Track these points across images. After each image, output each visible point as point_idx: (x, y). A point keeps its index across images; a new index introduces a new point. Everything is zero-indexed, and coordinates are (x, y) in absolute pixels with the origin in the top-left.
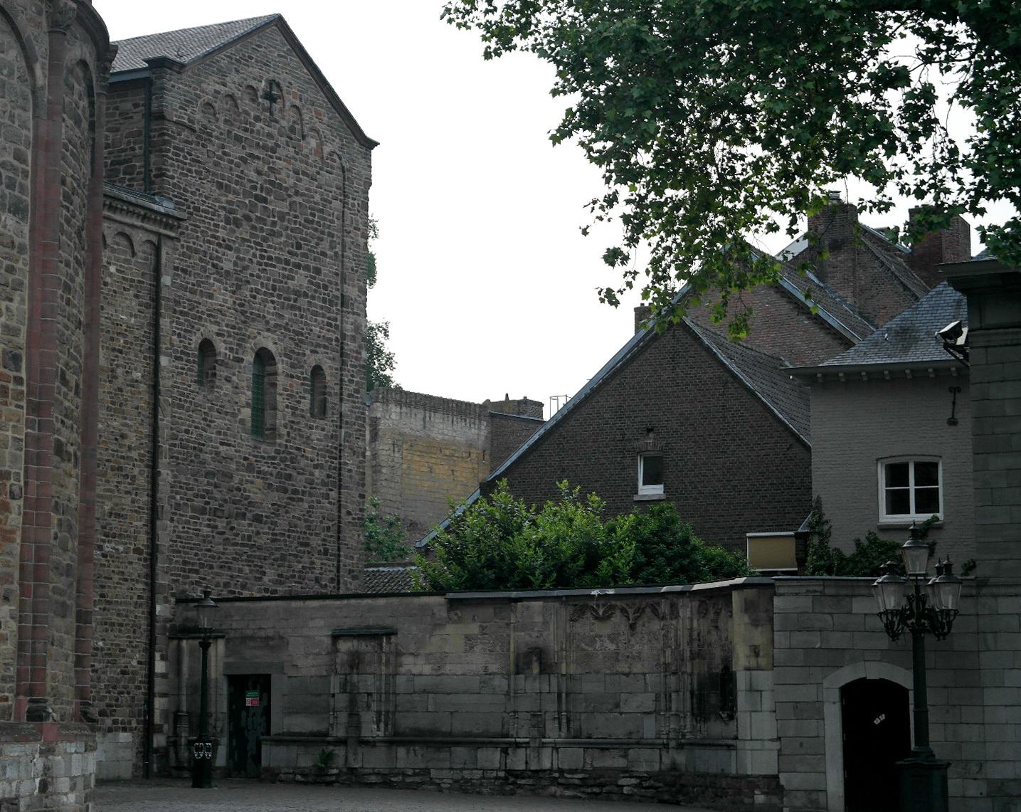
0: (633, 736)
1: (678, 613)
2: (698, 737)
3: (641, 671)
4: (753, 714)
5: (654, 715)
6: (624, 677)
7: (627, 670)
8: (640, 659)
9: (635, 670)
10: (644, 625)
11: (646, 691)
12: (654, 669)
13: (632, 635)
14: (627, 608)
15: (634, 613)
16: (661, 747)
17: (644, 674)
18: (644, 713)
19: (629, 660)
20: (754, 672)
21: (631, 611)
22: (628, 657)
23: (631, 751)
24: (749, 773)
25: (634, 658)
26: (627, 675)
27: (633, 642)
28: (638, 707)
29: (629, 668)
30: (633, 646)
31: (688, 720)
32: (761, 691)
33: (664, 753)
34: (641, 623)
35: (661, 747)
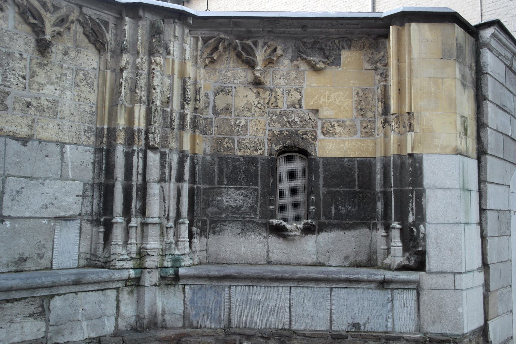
0: (28, 266)
1: (167, 48)
2: (196, 263)
3: (55, 138)
4: (466, 227)
5: (76, 224)
6: (15, 145)
7: (24, 132)
8: (56, 114)
9: (43, 135)
10: (66, 54)
11: (62, 177)
12: (83, 138)
13: (41, 65)
14: (42, 11)
15: (55, 25)
16: (119, 285)
17: (61, 144)
18: (56, 218)
19: (32, 111)
20: (466, 159)
21: (49, 19)
22: (29, 105)
23: (57, 303)
24: (466, 331)
25: (41, 109)
26: (24, 141)
27: (41, 77)
28: (45, 207)
29: (31, 127)
30: (41, 86)
31: (184, 230)
32: (470, 191)
33: (125, 296)
34: (60, 47)
35: (119, 285)
